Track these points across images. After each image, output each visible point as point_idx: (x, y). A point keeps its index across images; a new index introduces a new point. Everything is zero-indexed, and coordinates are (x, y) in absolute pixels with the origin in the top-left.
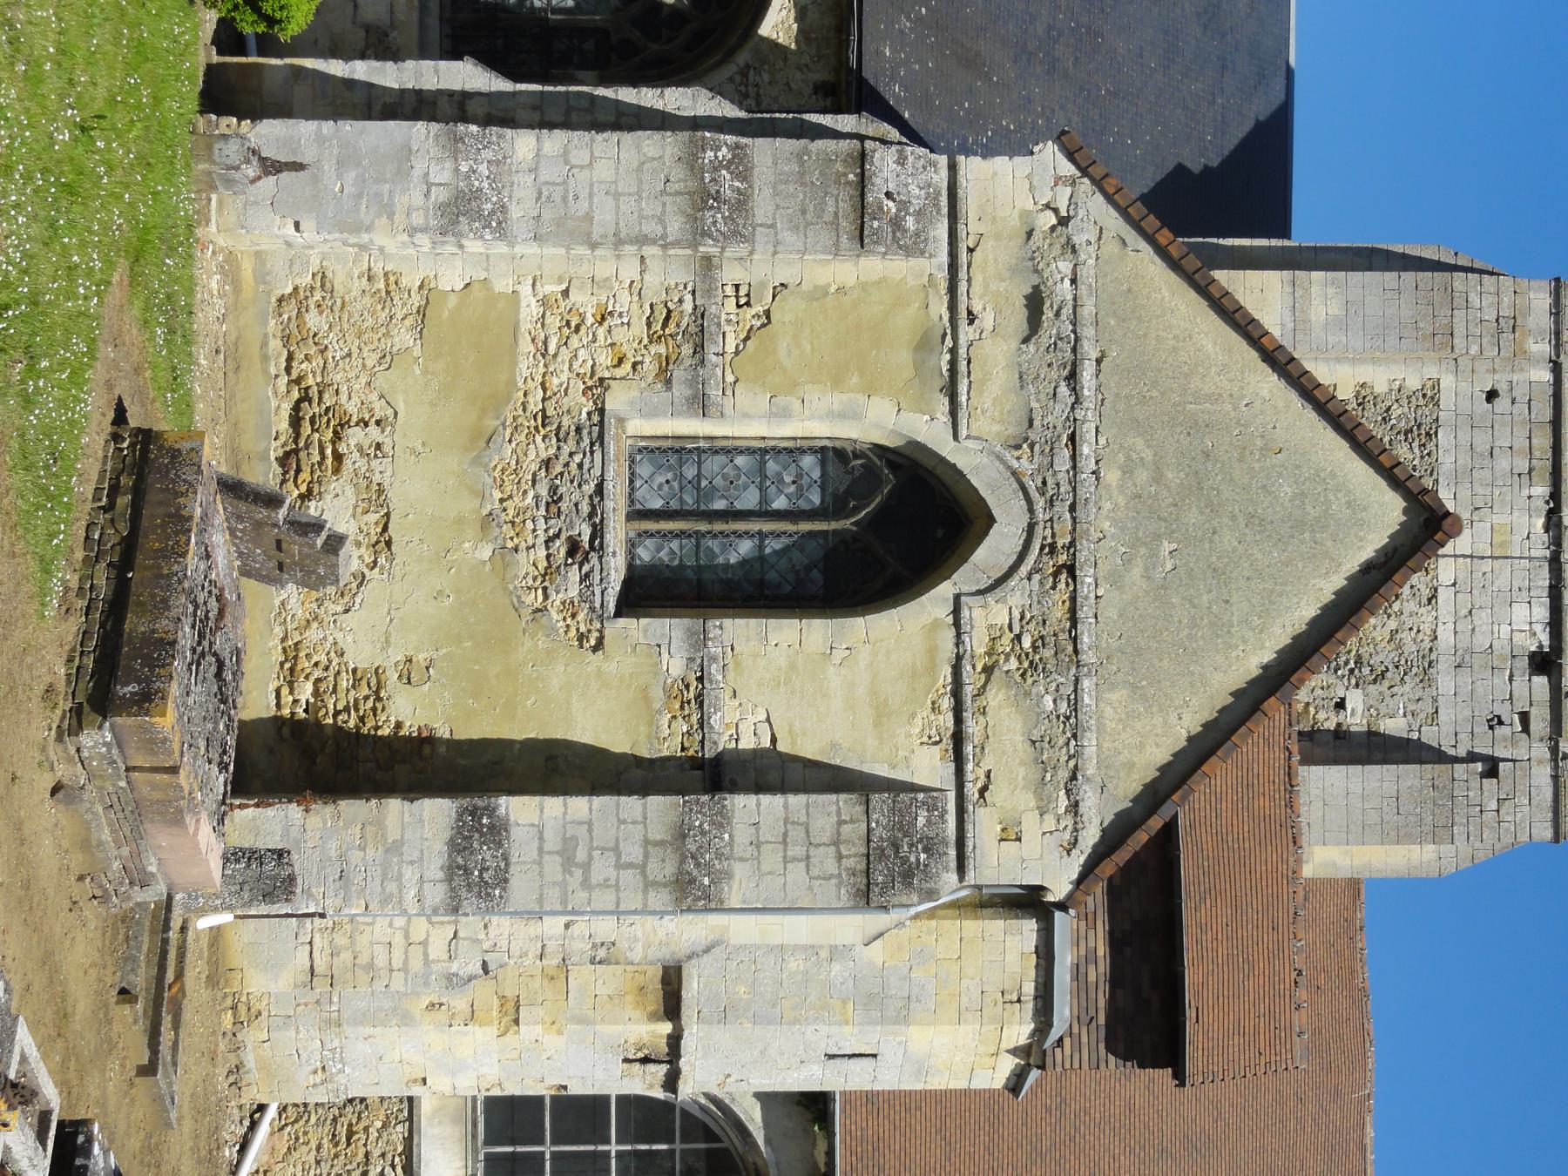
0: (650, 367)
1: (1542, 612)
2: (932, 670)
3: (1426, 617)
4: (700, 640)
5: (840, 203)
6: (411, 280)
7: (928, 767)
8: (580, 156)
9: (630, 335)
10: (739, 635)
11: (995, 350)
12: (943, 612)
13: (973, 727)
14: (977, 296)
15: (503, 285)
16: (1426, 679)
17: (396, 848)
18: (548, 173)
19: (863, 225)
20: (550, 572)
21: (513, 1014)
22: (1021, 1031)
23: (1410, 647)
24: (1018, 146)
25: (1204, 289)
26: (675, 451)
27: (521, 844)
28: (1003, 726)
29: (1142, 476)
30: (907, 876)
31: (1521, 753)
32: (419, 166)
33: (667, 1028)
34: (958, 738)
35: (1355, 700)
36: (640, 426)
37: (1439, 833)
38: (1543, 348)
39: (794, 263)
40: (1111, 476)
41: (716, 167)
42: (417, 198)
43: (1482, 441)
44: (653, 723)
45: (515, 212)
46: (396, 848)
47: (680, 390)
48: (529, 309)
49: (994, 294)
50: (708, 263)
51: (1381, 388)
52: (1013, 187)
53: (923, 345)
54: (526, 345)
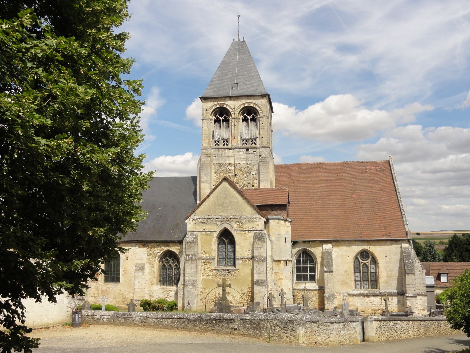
0: (209, 264)
1: (241, 150)
2: (241, 234)
3: (242, 164)
4: (238, 259)
5: (192, 244)
6: (201, 290)
7: (252, 234)
8: (188, 272)
9: (206, 267)
10: (237, 255)
11: (207, 227)
12: (235, 232)
13: (247, 229)
14: (202, 229)
15: (201, 280)
16: (250, 164)
17: (259, 291)
18: (190, 276)
19: (194, 242)
20: (231, 275)
21: (280, 279)
22: (282, 222)
23: (246, 166)
24: (186, 225)
25: (200, 205)
26: (219, 262)
27: (259, 278)
28: (247, 226)
29: (221, 211)
30: (262, 237)
31: (259, 152)
32: (189, 289)
33: (282, 262)
34: (248, 231)
35: (252, 173)
36: (216, 266)
37: (268, 163)
38: (209, 151)
39: (199, 250)
40: (221, 214)
41: (189, 258)
42: (192, 290)
43: (221, 158)
44: (247, 264)
45: (194, 279)
46: (259, 291)
47: (212, 261)
48: (204, 277)
49: (201, 227)
50: (199, 258)
51: (214, 171)
52: (190, 225)
53: (207, 235)
54: (208, 278)
